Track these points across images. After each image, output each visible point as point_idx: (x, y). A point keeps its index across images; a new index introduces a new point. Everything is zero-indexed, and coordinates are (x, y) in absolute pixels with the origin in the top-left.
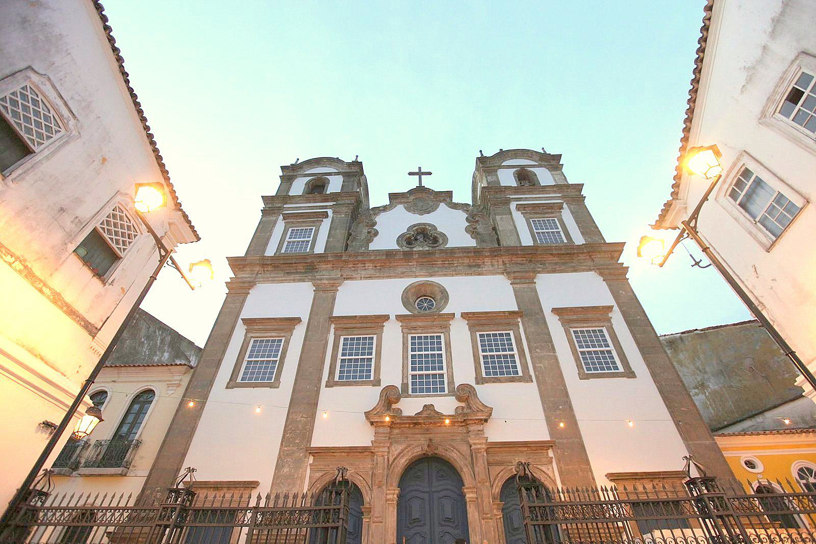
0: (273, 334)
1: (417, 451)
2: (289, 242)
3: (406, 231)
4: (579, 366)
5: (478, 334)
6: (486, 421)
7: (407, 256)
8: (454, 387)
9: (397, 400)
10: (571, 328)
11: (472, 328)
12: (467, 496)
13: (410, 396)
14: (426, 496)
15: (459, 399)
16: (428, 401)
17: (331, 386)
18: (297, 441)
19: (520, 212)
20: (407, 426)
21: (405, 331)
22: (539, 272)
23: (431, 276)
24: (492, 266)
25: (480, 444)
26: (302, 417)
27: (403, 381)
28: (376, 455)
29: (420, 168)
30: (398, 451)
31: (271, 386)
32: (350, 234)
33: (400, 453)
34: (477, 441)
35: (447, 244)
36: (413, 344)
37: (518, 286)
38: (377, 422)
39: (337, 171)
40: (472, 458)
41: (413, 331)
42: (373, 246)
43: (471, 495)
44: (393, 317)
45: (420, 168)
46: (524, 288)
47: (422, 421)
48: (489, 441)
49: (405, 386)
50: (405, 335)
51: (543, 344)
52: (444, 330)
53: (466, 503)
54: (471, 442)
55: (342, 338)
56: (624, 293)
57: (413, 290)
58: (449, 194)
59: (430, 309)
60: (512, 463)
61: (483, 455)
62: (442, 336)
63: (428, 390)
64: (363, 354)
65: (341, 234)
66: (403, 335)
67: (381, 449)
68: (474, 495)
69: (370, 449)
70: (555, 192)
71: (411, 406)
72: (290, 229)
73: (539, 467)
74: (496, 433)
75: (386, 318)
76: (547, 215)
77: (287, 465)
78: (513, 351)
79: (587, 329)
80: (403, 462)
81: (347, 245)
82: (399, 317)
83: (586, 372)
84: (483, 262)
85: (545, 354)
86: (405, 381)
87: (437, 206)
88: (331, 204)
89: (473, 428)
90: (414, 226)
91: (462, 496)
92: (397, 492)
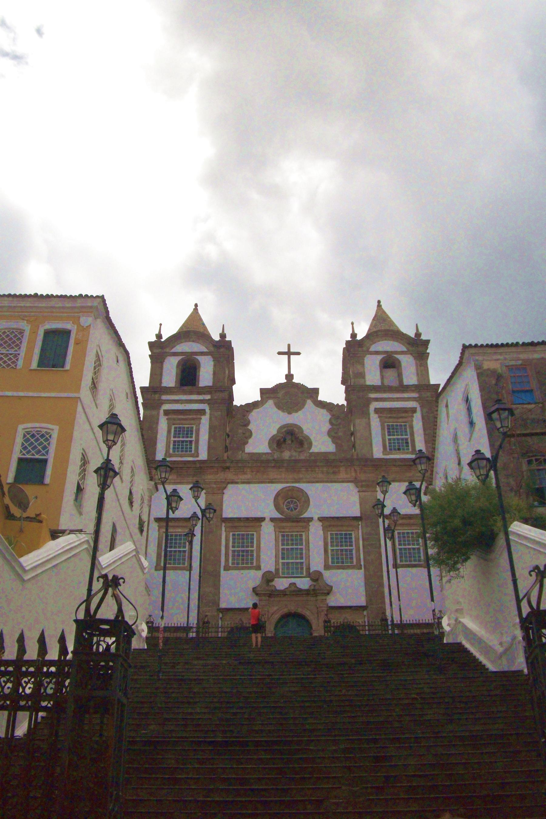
0: (180, 530)
2: (175, 442)
5: (329, 533)
6: (328, 594)
7: (278, 464)
9: (272, 580)
11: (325, 529)
15: (313, 580)
16: (293, 580)
17: (228, 570)
23: (298, 481)
29: (289, 346)
37: (363, 493)
42: (249, 449)
44: (267, 520)
45: (289, 346)
48: (329, 605)
49: (277, 570)
58: (316, 391)
62: (303, 534)
70: (413, 391)
71: (281, 584)
74: (334, 600)
75: (262, 519)
76: (400, 420)
78: (352, 547)
79: (407, 531)
80: (277, 616)
82: (272, 520)
84: (339, 471)
86: (277, 567)
88: (208, 397)
89: (320, 598)
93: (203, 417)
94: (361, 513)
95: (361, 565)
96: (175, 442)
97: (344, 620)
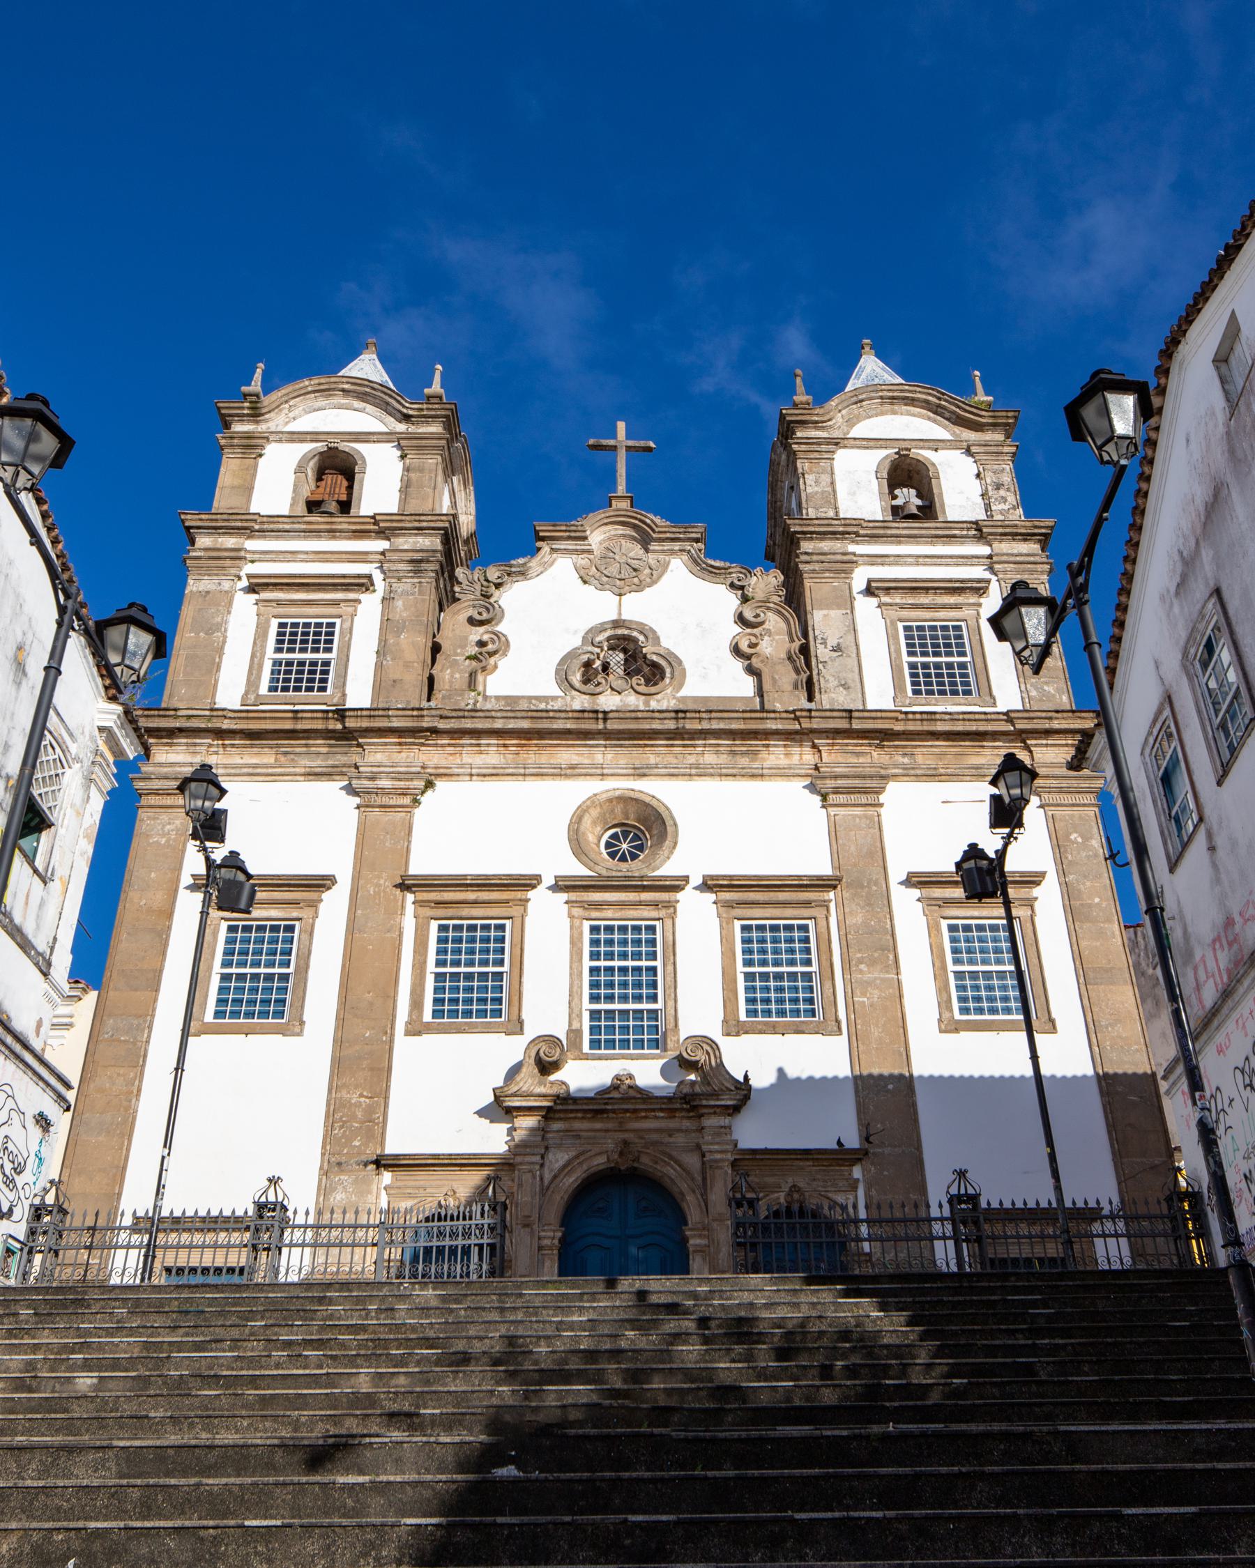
1: (600, 1162)
3: (579, 643)
4: (944, 1004)
6: (736, 1109)
10: (944, 918)
12: (692, 1242)
13: (587, 1057)
17: (419, 1033)
18: (357, 1143)
19: (873, 601)
20: (580, 1115)
21: (577, 912)
22: (895, 777)
23: (640, 772)
24: (787, 755)
26: (361, 1096)
27: (570, 1024)
30: (561, 1163)
31: (283, 1031)
32: (436, 649)
33: (565, 1166)
35: (681, 685)
36: (595, 943)
37: (842, 811)
39: (385, 429)
40: (704, 1179)
41: (595, 914)
43: (698, 1241)
46: (854, 817)
48: (741, 1145)
49: (574, 1034)
50: (577, 922)
51: (876, 955)
52: (662, 913)
53: (688, 1256)
54: (705, 1148)
55: (434, 925)
56: (1080, 840)
57: (595, 812)
59: (634, 857)
61: (726, 1173)
63: (625, 1044)
64: (485, 963)
65: (413, 645)
66: (572, 923)
67: (528, 1159)
68: (704, 1242)
72: (274, 623)
73: (830, 1195)
77: (340, 1188)
80: (571, 1181)
81: (431, 680)
83: (957, 1016)
85: (876, 975)
86: (576, 1026)
87: (665, 566)
89: (711, 1122)
90: (601, 628)
91: (685, 1240)
92: (559, 1234)
93: (364, 597)
94: (837, 865)
95: (838, 1022)
96: (277, 663)
97: (790, 1194)
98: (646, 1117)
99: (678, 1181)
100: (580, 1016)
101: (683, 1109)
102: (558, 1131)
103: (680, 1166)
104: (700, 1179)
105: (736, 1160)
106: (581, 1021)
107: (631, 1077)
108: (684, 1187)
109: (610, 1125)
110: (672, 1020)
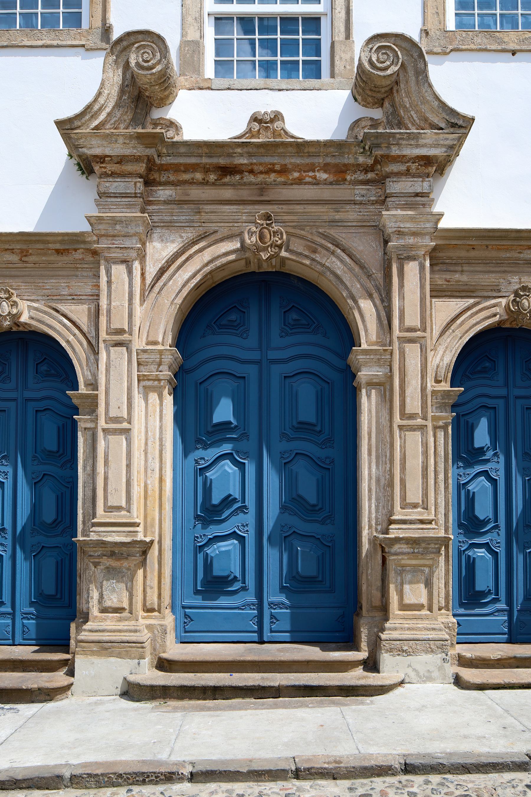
8: (352, 59)
14: (251, 371)
20: (199, 176)
25: (414, 234)
28: (107, 260)
34: (408, 225)
38: (101, 159)
47: (244, 161)
48: (443, 224)
54: (391, 226)
60: (499, 291)
67: (118, 242)
69: (84, 242)
86: (193, 35)
98: (299, 182)
99: (347, 278)
100: (199, 20)
101: (358, 167)
102: (166, 202)
103: (350, 256)
104: (379, 276)
105: (435, 249)
106: (201, 29)
107: (277, 116)
108: (356, 288)
109: (245, 194)
110: (342, 29)
